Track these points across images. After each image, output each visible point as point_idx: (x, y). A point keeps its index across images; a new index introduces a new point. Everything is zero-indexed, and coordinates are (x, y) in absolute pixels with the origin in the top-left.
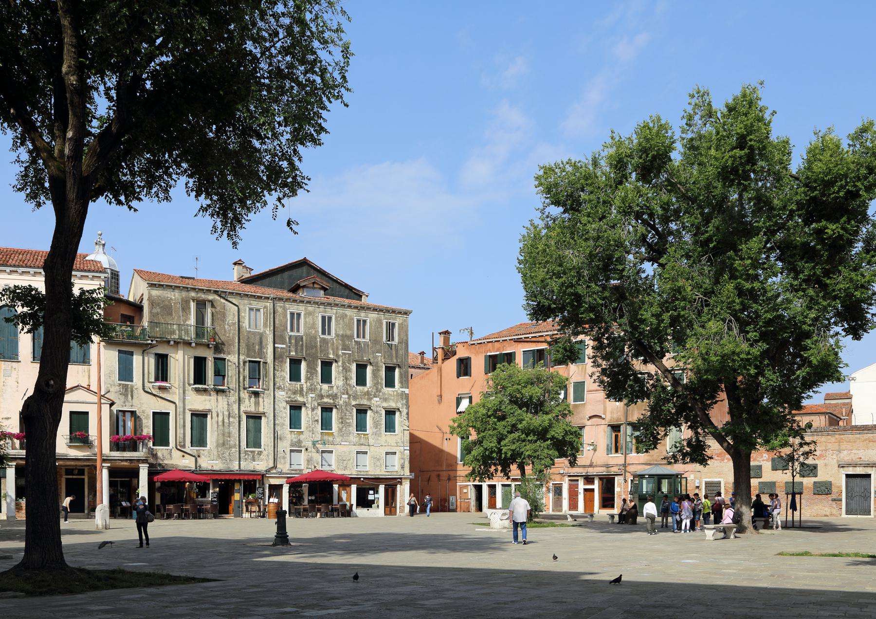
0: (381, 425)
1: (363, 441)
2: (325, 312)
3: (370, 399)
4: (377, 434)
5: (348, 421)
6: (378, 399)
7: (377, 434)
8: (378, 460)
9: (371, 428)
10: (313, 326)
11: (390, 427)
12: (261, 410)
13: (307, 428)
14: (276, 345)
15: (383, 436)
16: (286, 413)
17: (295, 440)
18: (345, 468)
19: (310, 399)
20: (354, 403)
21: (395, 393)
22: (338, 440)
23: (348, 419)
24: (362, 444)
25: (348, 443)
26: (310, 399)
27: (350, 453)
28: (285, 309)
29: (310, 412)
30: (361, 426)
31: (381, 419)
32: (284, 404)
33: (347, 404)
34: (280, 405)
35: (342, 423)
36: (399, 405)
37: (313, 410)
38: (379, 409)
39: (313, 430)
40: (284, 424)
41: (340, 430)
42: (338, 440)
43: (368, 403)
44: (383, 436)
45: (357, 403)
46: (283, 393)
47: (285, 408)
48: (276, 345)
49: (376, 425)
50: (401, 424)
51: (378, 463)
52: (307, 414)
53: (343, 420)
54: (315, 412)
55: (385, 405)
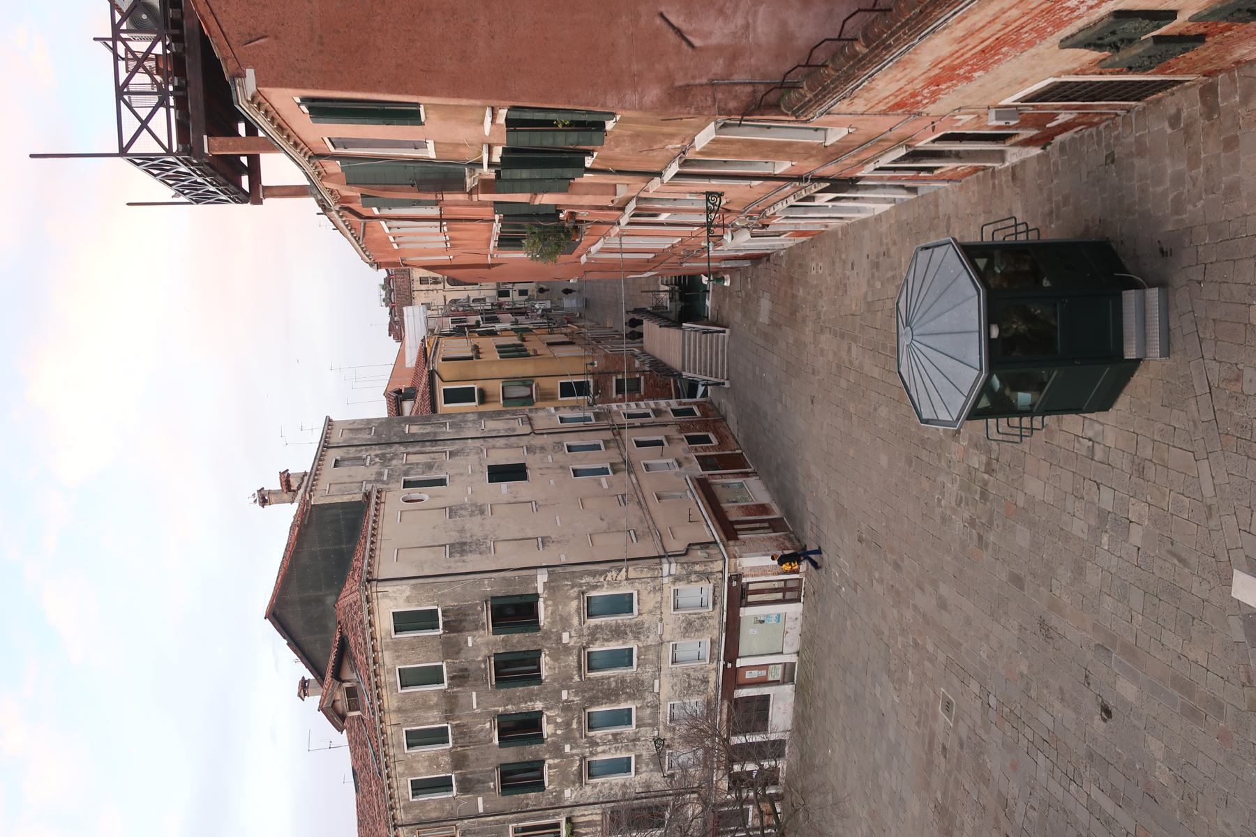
0: (618, 626)
1: (651, 656)
2: (400, 744)
3: (567, 649)
4: (638, 631)
5: (613, 685)
6: (565, 637)
7: (638, 631)
8: (690, 624)
9: (624, 643)
10: (433, 760)
11: (622, 604)
12: (598, 818)
13: (629, 750)
14: (481, 810)
15: (640, 618)
16: (603, 784)
17: (651, 766)
18: (705, 681)
19: (574, 751)
20: (577, 678)
21: (550, 603)
22: (650, 699)
23: (609, 684)
24: (659, 657)
25: (657, 682)
26: (574, 751)
27: (673, 675)
28: (408, 808)
29: (600, 749)
30: (624, 658)
31: (607, 625)
32: (588, 789)
33: (579, 690)
34: (589, 794)
35: (617, 695)
36: (574, 592)
37: (593, 743)
38: (586, 632)
39: (634, 740)
40: (624, 785)
41: (631, 697)
42: (650, 699)
43: (575, 651)
44: (640, 618)
45: (575, 673)
46: (567, 793)
47: (595, 786)
48: (481, 810)
49: (618, 632)
50: (614, 583)
51: (697, 623)
52: (604, 752)
53: (611, 694)
54: (598, 741)
55: (575, 621)
